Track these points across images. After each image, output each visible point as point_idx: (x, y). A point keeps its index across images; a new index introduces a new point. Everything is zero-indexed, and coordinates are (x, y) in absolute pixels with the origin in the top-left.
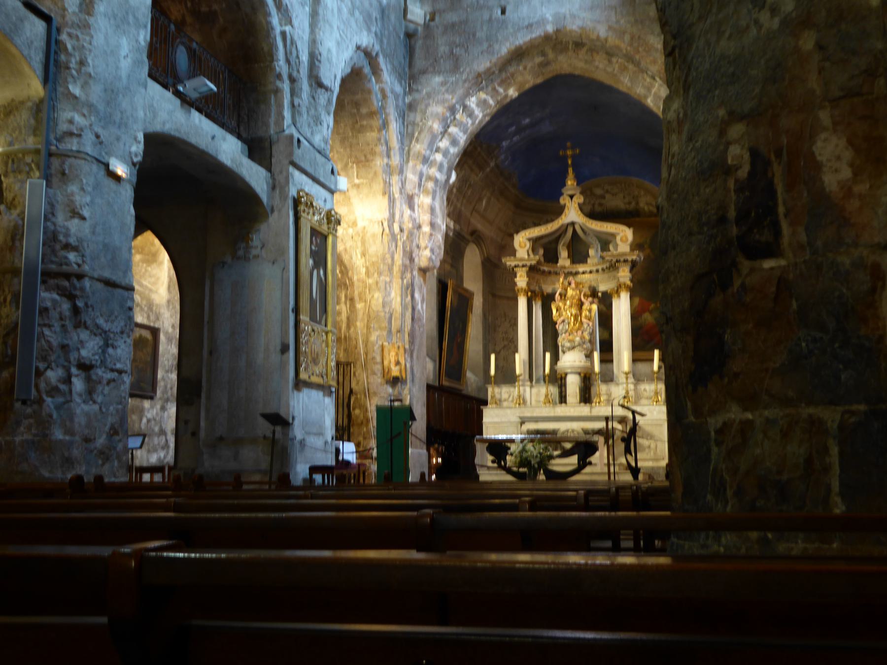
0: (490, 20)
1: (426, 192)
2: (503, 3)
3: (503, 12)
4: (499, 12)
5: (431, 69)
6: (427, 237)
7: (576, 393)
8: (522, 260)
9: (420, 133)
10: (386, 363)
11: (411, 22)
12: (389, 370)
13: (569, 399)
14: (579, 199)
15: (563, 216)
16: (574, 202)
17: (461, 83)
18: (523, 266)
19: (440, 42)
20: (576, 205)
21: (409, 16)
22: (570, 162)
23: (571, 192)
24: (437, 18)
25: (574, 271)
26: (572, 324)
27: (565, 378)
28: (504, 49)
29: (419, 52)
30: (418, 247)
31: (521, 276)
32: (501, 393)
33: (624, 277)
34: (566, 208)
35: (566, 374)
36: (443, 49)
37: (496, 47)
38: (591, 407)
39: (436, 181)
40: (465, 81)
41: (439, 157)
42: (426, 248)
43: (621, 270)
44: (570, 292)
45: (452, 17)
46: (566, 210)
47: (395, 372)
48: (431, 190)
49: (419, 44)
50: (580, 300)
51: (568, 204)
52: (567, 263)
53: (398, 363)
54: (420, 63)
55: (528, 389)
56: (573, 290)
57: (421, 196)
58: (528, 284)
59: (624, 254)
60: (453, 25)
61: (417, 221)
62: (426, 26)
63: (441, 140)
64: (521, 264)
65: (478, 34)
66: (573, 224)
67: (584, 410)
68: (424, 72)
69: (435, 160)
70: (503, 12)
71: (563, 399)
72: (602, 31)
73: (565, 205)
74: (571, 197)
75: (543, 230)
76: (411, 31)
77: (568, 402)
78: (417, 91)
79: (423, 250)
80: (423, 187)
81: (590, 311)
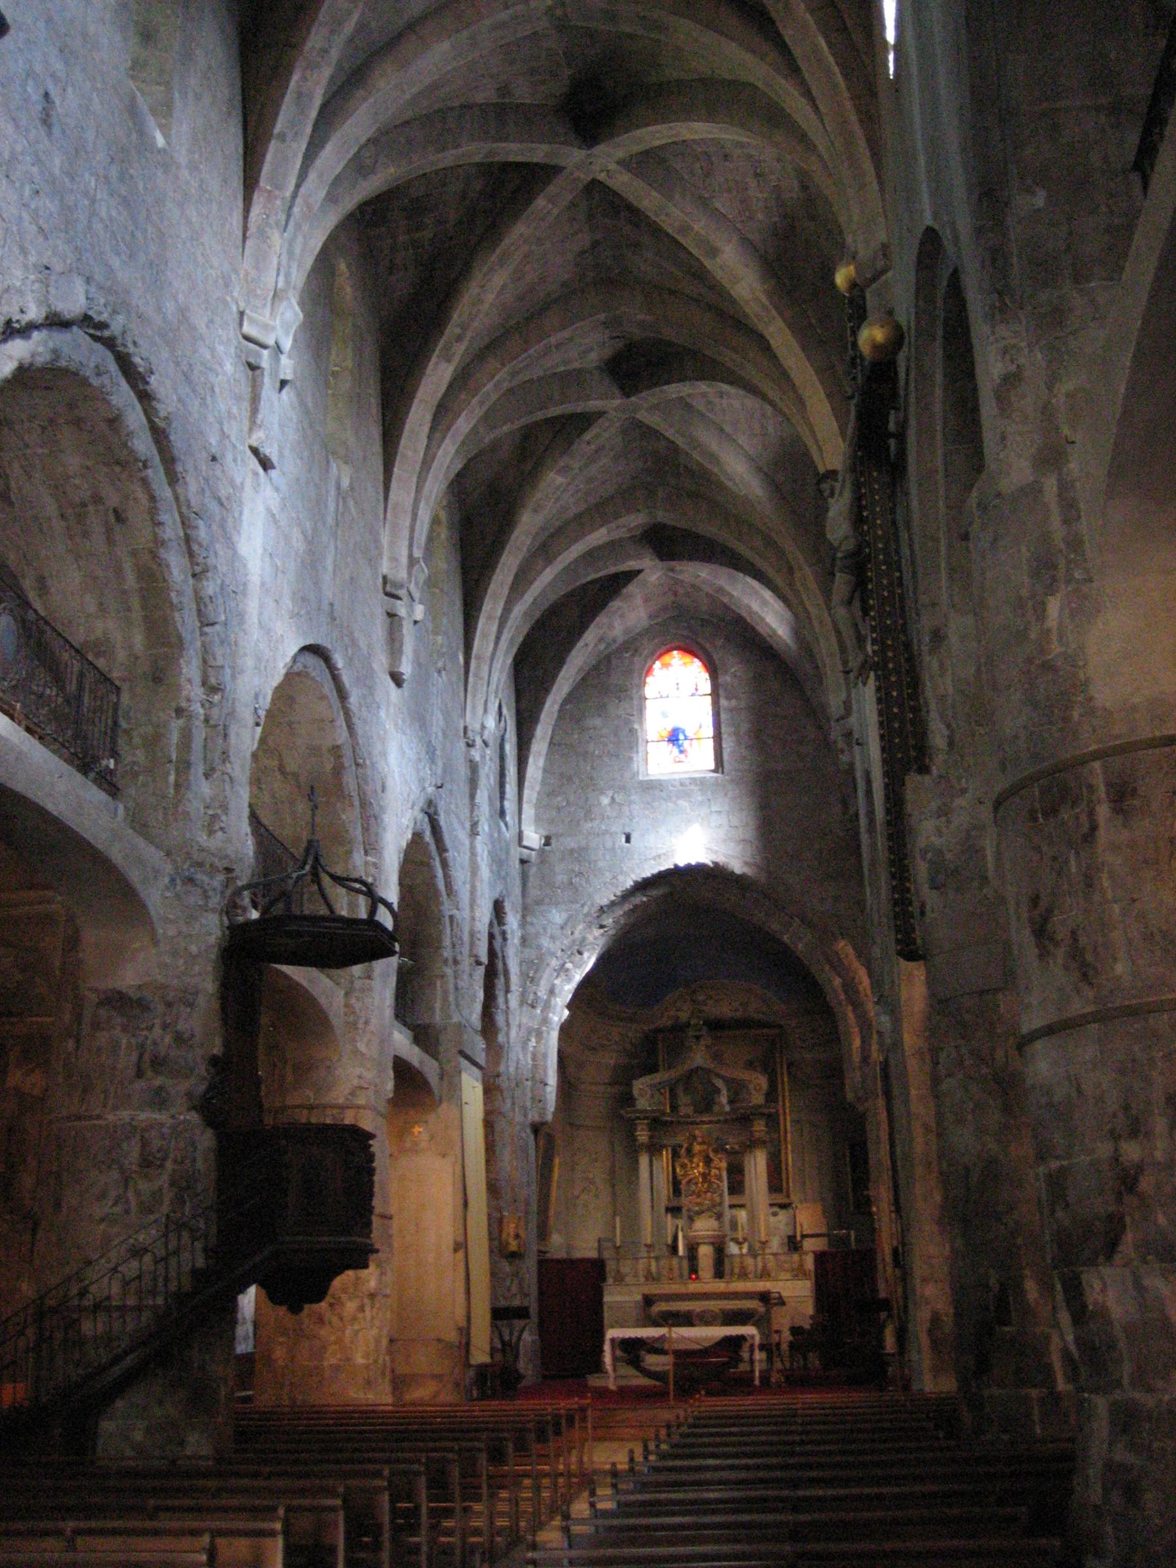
0: (613, 849)
2: (627, 830)
3: (628, 840)
4: (623, 839)
5: (547, 900)
8: (642, 1112)
9: (535, 972)
10: (504, 1236)
11: (526, 847)
12: (508, 1243)
17: (581, 917)
18: (646, 1118)
19: (557, 869)
21: (525, 843)
24: (553, 841)
25: (698, 1120)
27: (696, 1250)
28: (629, 884)
29: (533, 881)
31: (643, 1130)
33: (760, 1131)
35: (698, 1244)
36: (561, 878)
37: (621, 878)
40: (586, 915)
43: (756, 1123)
44: (697, 1148)
45: (570, 843)
47: (513, 1245)
49: (533, 870)
52: (690, 1110)
53: (517, 1236)
54: (534, 892)
56: (700, 1144)
58: (651, 1137)
59: (760, 1106)
60: (572, 851)
62: (541, 852)
64: (642, 1116)
65: (601, 864)
67: (720, 1286)
68: (539, 903)
70: (628, 840)
71: (694, 1269)
72: (737, 867)
74: (698, 1038)
76: (525, 857)
78: (532, 924)
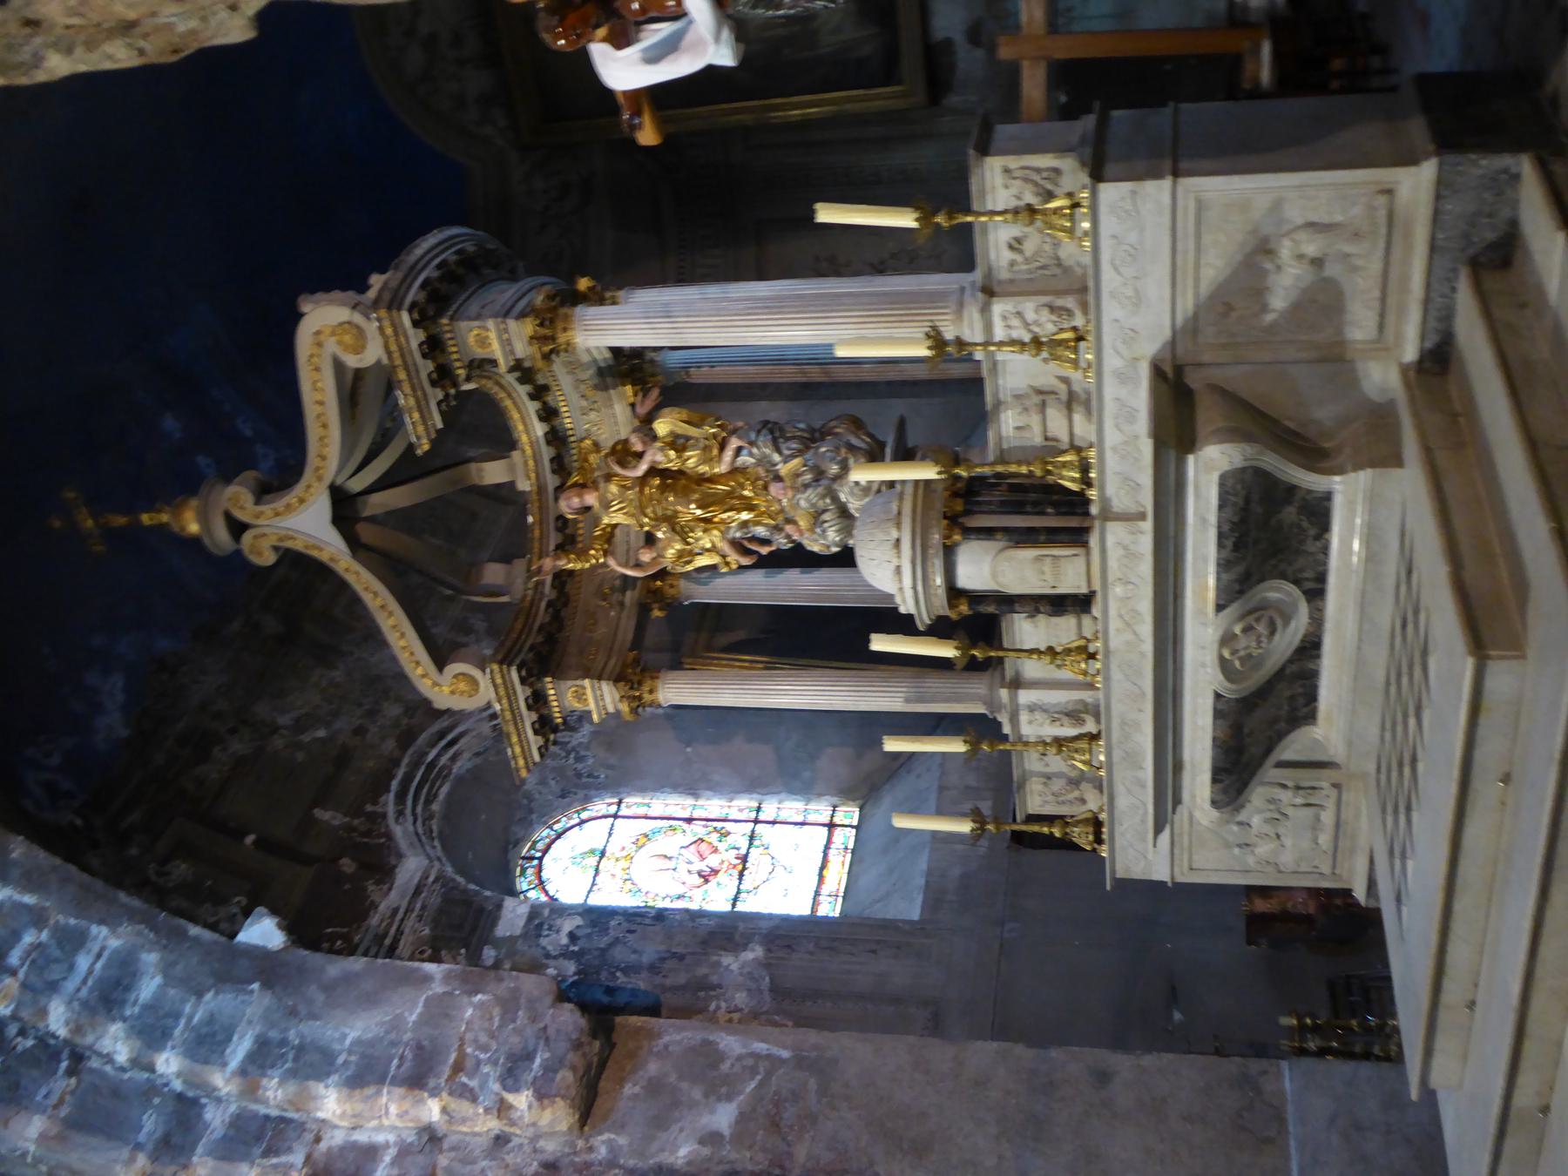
1: (302, 1101)
6: (463, 1107)
7: (1039, 559)
13: (1071, 581)
14: (238, 497)
15: (324, 557)
16: (257, 516)
20: (266, 509)
22: (120, 520)
23: (222, 534)
26: (745, 516)
30: (501, 1140)
31: (580, 696)
32: (1048, 777)
34: (289, 544)
35: (955, 593)
38: (1107, 515)
39: (262, 1057)
41: (169, 1063)
42: (503, 1109)
46: (298, 545)
48: (292, 1087)
50: (643, 481)
51: (273, 541)
55: (1025, 696)
56: (606, 505)
57: (321, 1115)
61: (411, 1138)
63: (108, 1058)
66: (344, 508)
69: (179, 1075)
73: (276, 549)
74: (238, 528)
75: (391, 622)
77: (1084, 590)
79: (512, 1123)
80: (286, 1110)
81: (678, 443)
